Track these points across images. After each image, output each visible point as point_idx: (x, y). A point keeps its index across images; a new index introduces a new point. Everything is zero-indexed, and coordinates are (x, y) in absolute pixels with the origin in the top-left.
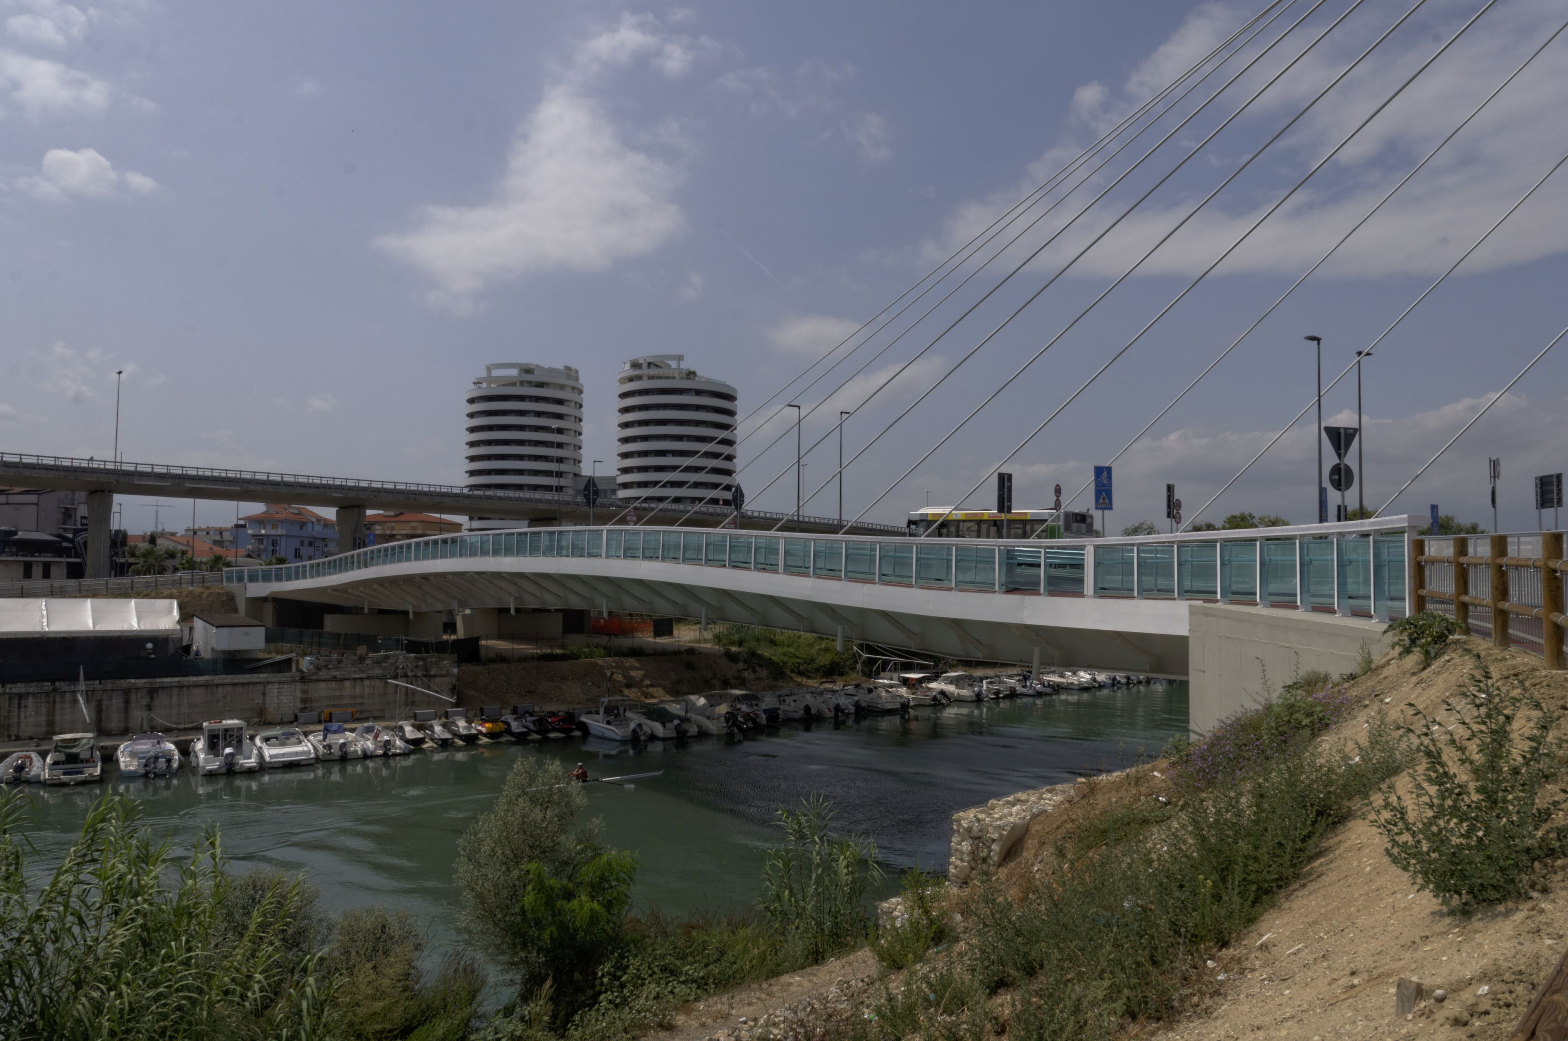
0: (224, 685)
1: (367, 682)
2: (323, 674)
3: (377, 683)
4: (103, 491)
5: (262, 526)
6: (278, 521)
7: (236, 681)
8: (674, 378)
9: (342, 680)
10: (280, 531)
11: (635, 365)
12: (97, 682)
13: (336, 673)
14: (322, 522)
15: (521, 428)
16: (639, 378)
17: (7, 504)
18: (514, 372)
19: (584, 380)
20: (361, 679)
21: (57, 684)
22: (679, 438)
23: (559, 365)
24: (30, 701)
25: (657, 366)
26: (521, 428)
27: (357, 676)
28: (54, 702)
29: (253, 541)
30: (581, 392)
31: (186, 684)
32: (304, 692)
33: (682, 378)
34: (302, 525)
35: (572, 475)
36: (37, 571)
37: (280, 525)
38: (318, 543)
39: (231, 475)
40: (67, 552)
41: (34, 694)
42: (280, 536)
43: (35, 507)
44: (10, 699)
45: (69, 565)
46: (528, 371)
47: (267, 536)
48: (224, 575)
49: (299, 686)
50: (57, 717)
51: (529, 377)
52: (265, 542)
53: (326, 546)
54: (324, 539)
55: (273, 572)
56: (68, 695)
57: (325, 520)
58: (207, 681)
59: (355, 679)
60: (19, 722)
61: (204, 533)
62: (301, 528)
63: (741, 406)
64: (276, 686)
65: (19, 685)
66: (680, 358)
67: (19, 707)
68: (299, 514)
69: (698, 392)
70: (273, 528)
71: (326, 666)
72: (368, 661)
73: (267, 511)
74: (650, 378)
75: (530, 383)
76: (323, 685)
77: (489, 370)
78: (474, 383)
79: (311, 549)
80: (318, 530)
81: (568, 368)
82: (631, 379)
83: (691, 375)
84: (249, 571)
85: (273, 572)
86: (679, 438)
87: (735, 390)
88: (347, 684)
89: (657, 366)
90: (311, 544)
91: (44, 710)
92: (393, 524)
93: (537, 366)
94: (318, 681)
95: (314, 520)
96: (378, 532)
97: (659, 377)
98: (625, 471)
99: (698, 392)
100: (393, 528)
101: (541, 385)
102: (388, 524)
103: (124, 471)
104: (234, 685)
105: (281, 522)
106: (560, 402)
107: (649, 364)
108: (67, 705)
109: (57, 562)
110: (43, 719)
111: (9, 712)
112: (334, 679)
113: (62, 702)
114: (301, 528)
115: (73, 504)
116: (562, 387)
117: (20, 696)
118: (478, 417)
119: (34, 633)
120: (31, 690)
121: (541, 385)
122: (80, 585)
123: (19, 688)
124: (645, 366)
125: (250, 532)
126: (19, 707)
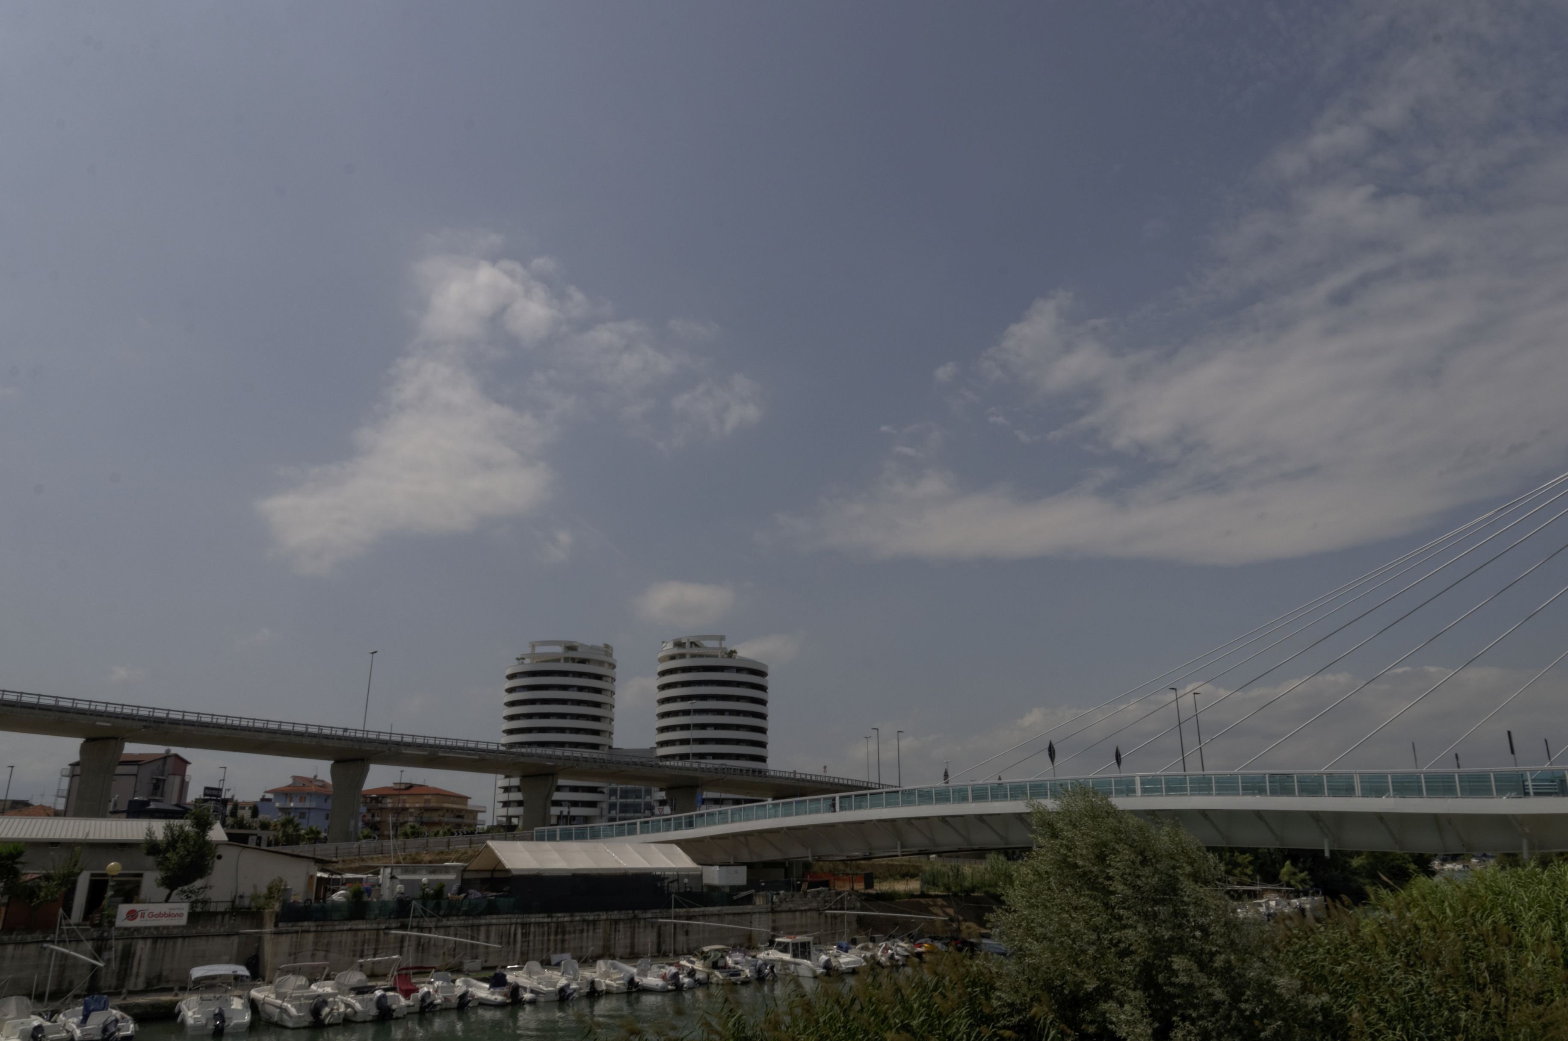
0: (728, 914)
1: (809, 913)
2: (784, 906)
3: (815, 914)
4: (362, 760)
7: (735, 911)
8: (717, 656)
9: (795, 911)
10: (307, 804)
11: (679, 644)
12: (658, 911)
13: (791, 905)
15: (564, 702)
16: (682, 656)
18: (559, 650)
19: (618, 656)
20: (805, 911)
21: (636, 912)
22: (721, 712)
23: (600, 644)
24: (621, 926)
25: (696, 645)
26: (564, 702)
27: (803, 908)
28: (634, 928)
29: (280, 814)
30: (613, 666)
31: (707, 913)
32: (774, 921)
33: (723, 657)
35: (607, 748)
39: (460, 744)
41: (623, 920)
42: (309, 809)
43: (133, 778)
44: (611, 925)
46: (571, 648)
47: (295, 809)
48: (535, 834)
49: (770, 916)
50: (636, 940)
51: (572, 654)
55: (546, 833)
56: (642, 922)
58: (719, 911)
59: (802, 911)
60: (615, 944)
62: (326, 801)
63: (770, 681)
64: (757, 916)
65: (616, 912)
66: (722, 638)
67: (615, 932)
69: (739, 670)
71: (785, 899)
72: (809, 896)
73: (294, 783)
74: (693, 656)
75: (573, 660)
76: (784, 915)
77: (533, 646)
78: (518, 659)
81: (607, 646)
82: (673, 658)
83: (731, 654)
84: (561, 830)
85: (546, 833)
86: (721, 712)
87: (766, 667)
88: (798, 914)
89: (696, 645)
91: (629, 934)
93: (580, 644)
94: (781, 912)
96: (390, 805)
97: (700, 656)
98: (662, 744)
99: (739, 670)
100: (405, 802)
101: (583, 661)
103: (381, 740)
104: (734, 914)
105: (310, 794)
106: (599, 677)
107: (692, 643)
108: (642, 930)
110: (628, 941)
111: (610, 934)
112: (790, 911)
113: (639, 927)
114: (326, 801)
115: (163, 775)
116: (601, 663)
117: (616, 922)
118: (519, 691)
119: (620, 869)
120: (622, 917)
121: (583, 661)
122: (405, 844)
123: (615, 915)
124: (688, 645)
125: (277, 805)
126: (615, 932)
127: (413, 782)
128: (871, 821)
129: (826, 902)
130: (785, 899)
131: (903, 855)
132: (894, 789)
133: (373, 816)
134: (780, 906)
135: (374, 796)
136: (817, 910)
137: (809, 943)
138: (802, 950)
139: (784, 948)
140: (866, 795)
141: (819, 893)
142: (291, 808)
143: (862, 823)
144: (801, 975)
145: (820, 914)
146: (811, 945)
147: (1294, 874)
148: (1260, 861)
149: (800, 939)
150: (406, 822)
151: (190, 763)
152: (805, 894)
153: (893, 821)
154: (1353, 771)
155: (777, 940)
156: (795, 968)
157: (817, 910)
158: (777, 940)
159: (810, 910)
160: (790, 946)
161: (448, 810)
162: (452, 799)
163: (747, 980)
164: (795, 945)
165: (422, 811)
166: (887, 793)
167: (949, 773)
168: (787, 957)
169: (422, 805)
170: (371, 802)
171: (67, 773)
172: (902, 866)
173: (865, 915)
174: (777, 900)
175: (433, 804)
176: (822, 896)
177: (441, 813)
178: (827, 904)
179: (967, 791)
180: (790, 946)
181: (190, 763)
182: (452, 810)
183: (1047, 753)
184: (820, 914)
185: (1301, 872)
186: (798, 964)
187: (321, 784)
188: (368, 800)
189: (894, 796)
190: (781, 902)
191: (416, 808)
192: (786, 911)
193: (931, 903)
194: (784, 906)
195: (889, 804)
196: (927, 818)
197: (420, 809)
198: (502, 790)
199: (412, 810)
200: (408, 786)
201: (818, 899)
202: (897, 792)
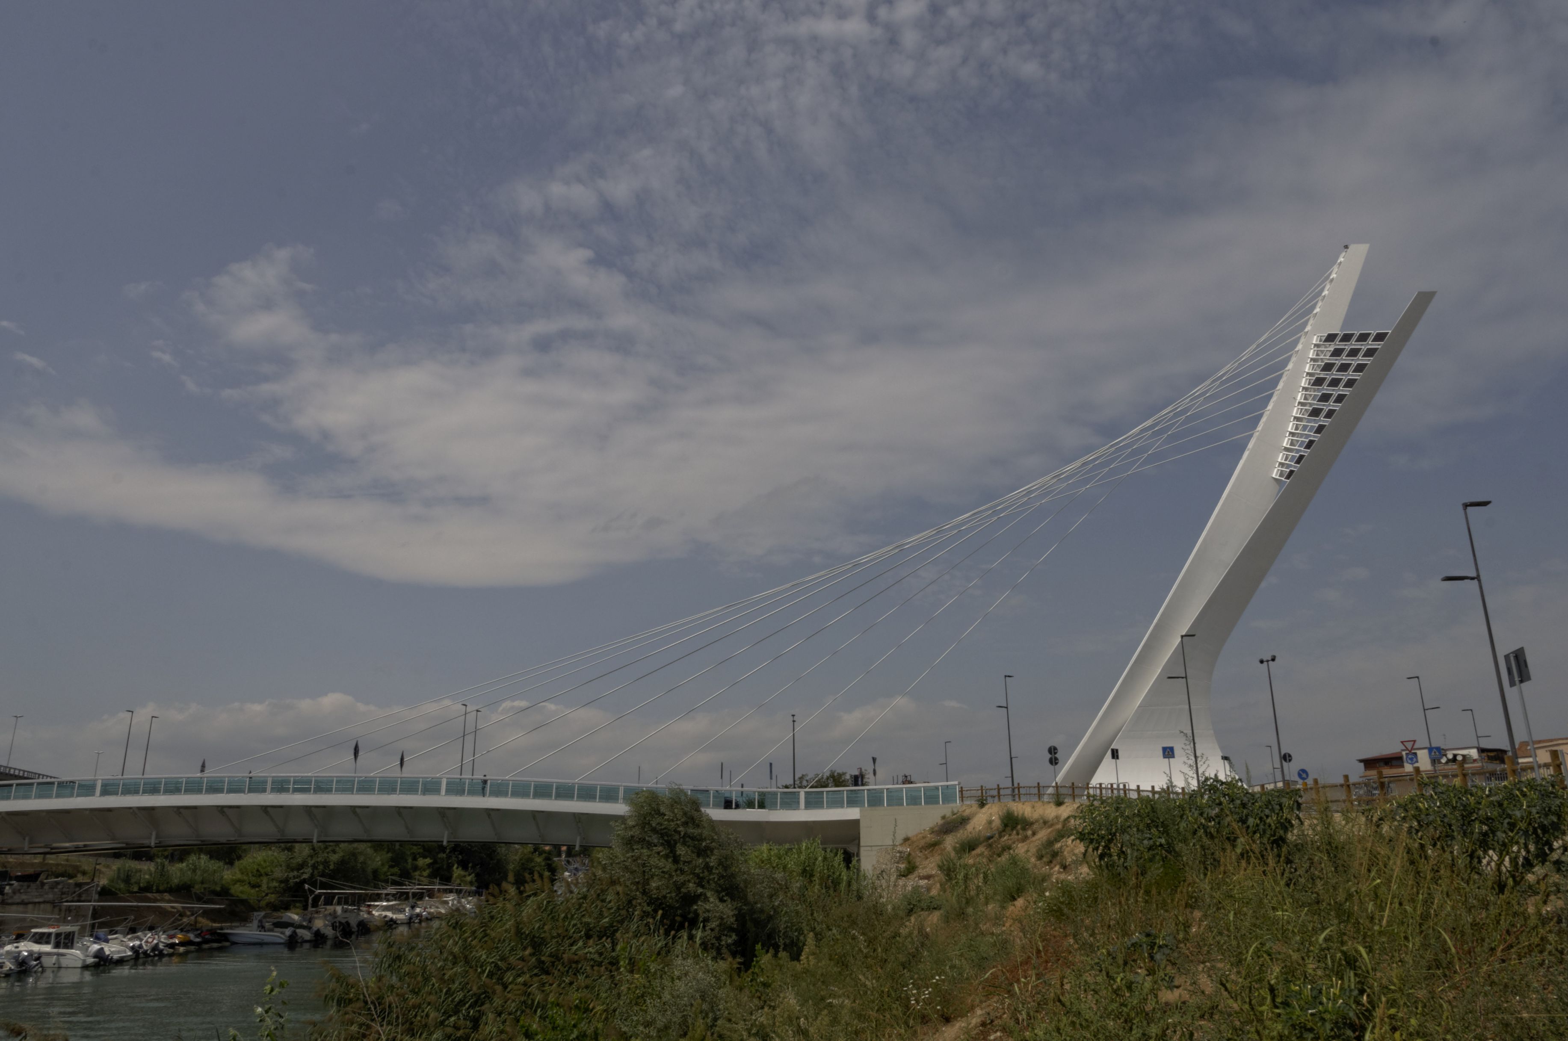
1: (42, 906)
2: (17, 898)
20: (39, 903)
27: (37, 900)
59: (35, 903)
71: (19, 890)
72: (46, 887)
88: (30, 907)
128: (130, 808)
129: (63, 893)
130: (19, 890)
131: (156, 847)
132: (49, 780)
134: (12, 897)
136: (52, 903)
137: (74, 933)
138: (66, 941)
139: (41, 939)
140: (11, 785)
141: (57, 883)
143: (109, 810)
144: (64, 965)
145: (54, 907)
146: (76, 935)
147: (465, 876)
148: (437, 866)
149: (68, 928)
152: (43, 884)
153: (152, 809)
154: (619, 784)
155: (34, 930)
156: (58, 960)
157: (52, 903)
158: (34, 930)
159: (44, 902)
160: (53, 937)
163: (10, 972)
164: (58, 935)
166: (39, 784)
167: (207, 765)
168: (47, 948)
172: (58, 865)
173: (102, 906)
174: (10, 891)
176: (60, 887)
178: (64, 896)
179: (266, 782)
180: (53, 937)
183: (352, 752)
184: (54, 907)
185: (469, 875)
186: (63, 955)
189: (47, 787)
190: (14, 892)
192: (18, 904)
193: (159, 898)
194: (17, 898)
195: (40, 796)
196: (195, 808)
201: (56, 890)
202: (53, 783)
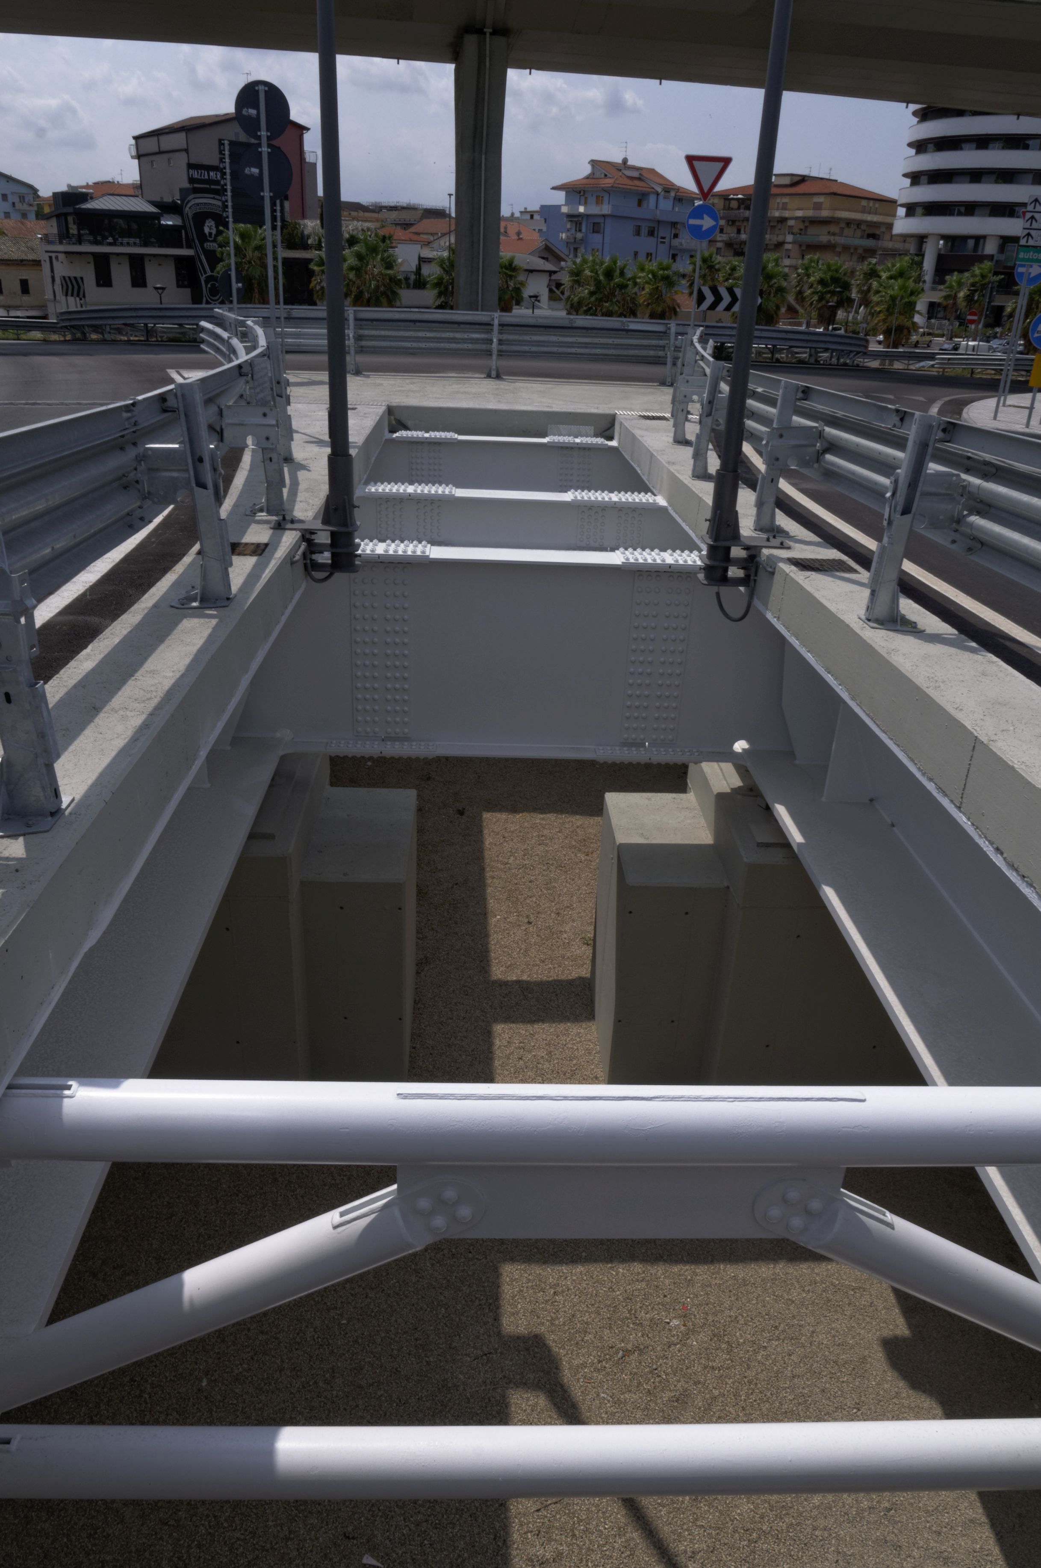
5: (583, 199)
6: (604, 190)
10: (606, 209)
14: (673, 194)
17: (160, 153)
29: (569, 226)
34: (641, 198)
36: (121, 273)
37: (606, 199)
38: (664, 232)
40: (170, 237)
42: (604, 216)
43: (184, 154)
45: (179, 260)
52: (584, 230)
53: (676, 236)
54: (674, 224)
57: (678, 189)
61: (528, 217)
68: (640, 179)
70: (597, 203)
73: (593, 173)
79: (652, 241)
80: (666, 205)
90: (651, 233)
92: (786, 200)
95: (659, 189)
100: (785, 207)
102: (779, 200)
105: (607, 191)
109: (154, 256)
127: (814, 174)
133: (739, 232)
135: (740, 196)
142: (580, 215)
150: (783, 243)
151: (308, 129)
161: (849, 223)
162: (864, 203)
165: (807, 224)
169: (810, 213)
170: (739, 208)
171: (134, 153)
175: (825, 213)
177: (834, 228)
181: (308, 129)
182: (859, 224)
187: (636, 174)
188: (734, 204)
191: (796, 218)
197: (803, 220)
198: (908, 181)
199: (791, 223)
200: (796, 179)
